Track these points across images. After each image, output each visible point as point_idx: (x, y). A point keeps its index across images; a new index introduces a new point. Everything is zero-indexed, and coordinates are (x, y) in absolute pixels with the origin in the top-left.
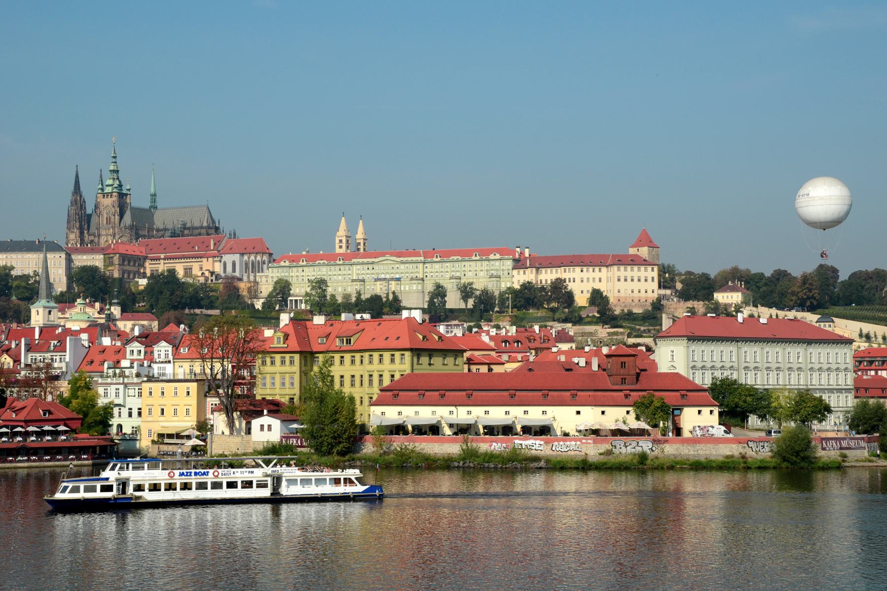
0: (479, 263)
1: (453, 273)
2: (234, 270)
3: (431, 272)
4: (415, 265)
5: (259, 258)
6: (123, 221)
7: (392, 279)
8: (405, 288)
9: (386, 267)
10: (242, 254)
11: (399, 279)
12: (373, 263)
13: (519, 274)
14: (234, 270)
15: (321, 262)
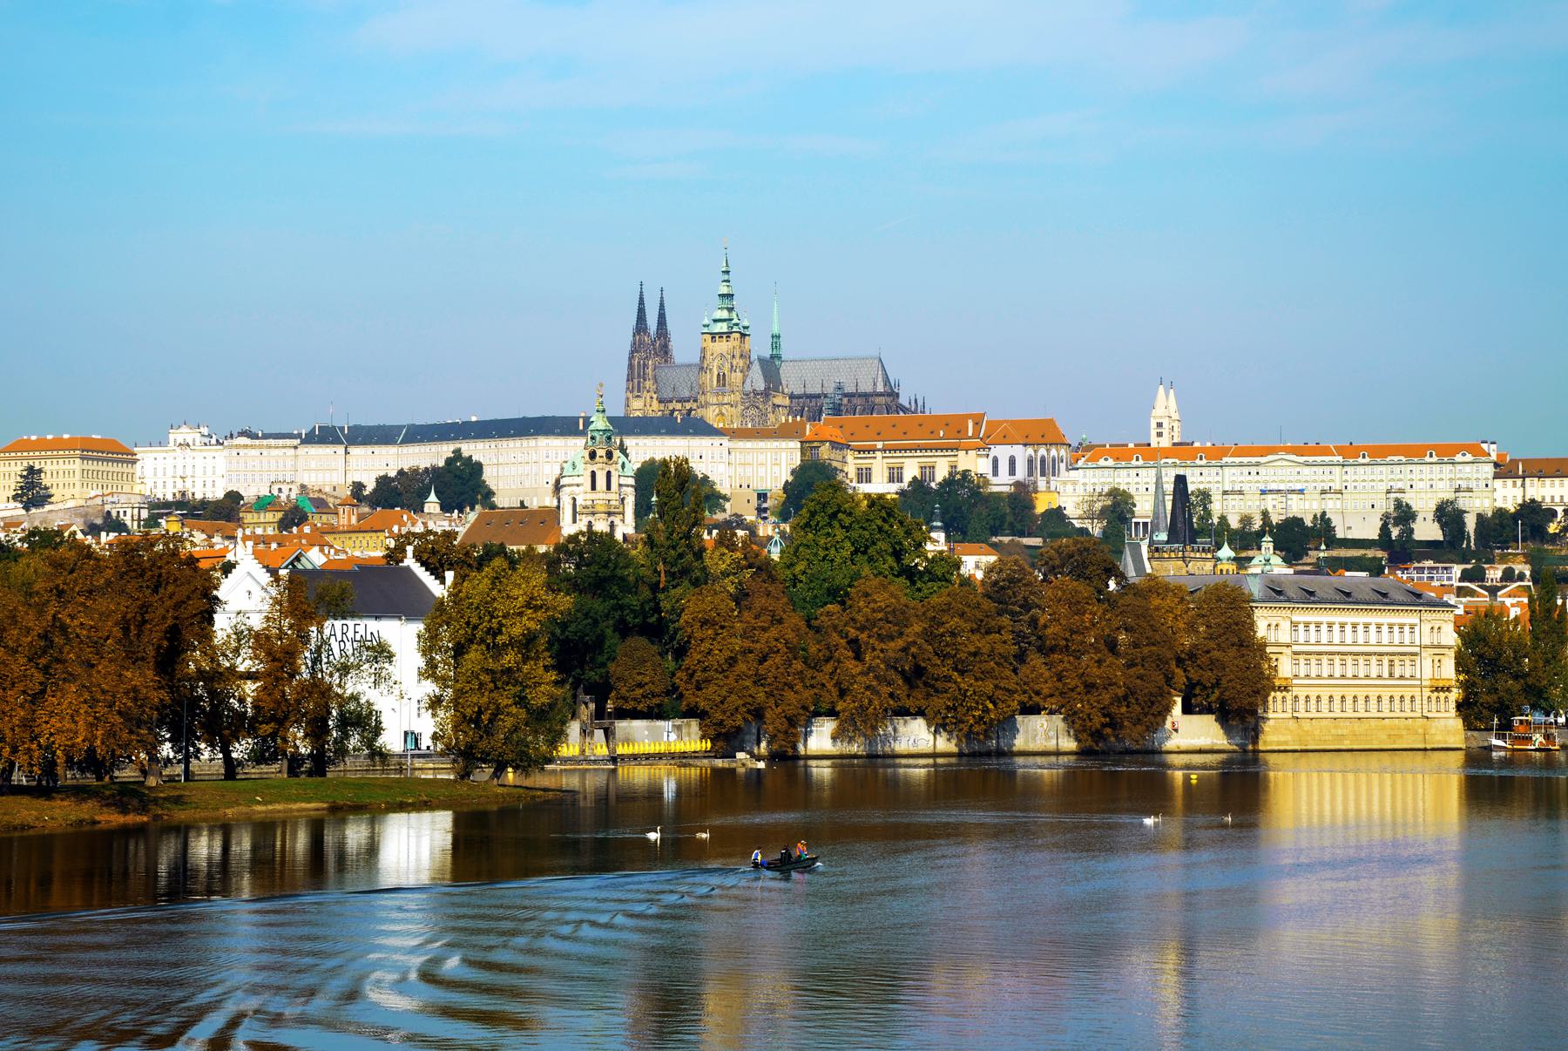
0: (1436, 468)
1: (1392, 483)
2: (1012, 472)
3: (1355, 481)
4: (1327, 469)
5: (1054, 452)
6: (748, 381)
7: (1293, 491)
8: (1311, 505)
9: (1279, 471)
10: (1025, 445)
11: (1301, 492)
12: (1258, 464)
13: (1505, 486)
14: (1012, 472)
15: (1170, 461)
